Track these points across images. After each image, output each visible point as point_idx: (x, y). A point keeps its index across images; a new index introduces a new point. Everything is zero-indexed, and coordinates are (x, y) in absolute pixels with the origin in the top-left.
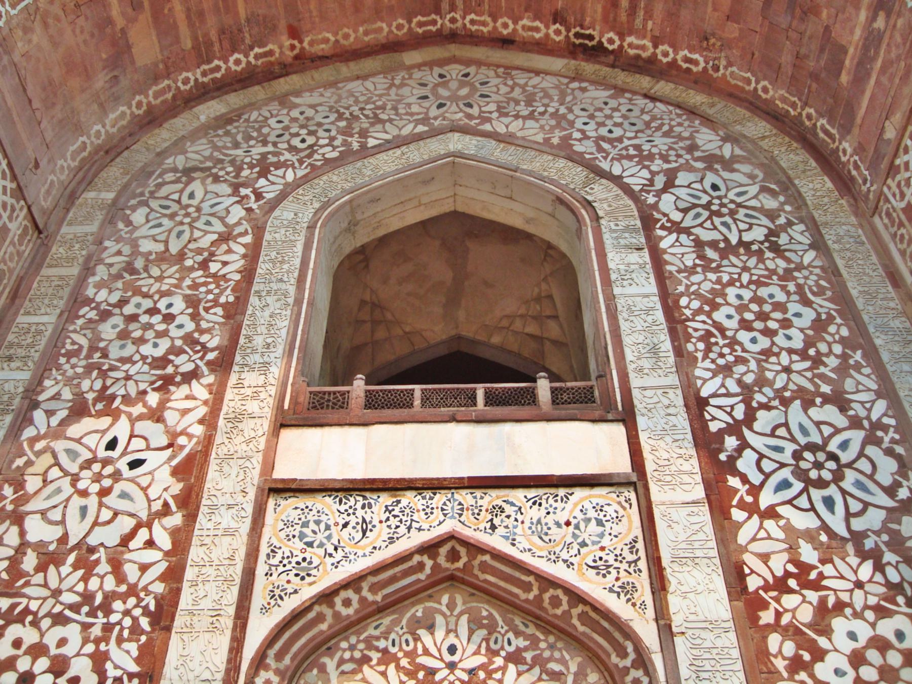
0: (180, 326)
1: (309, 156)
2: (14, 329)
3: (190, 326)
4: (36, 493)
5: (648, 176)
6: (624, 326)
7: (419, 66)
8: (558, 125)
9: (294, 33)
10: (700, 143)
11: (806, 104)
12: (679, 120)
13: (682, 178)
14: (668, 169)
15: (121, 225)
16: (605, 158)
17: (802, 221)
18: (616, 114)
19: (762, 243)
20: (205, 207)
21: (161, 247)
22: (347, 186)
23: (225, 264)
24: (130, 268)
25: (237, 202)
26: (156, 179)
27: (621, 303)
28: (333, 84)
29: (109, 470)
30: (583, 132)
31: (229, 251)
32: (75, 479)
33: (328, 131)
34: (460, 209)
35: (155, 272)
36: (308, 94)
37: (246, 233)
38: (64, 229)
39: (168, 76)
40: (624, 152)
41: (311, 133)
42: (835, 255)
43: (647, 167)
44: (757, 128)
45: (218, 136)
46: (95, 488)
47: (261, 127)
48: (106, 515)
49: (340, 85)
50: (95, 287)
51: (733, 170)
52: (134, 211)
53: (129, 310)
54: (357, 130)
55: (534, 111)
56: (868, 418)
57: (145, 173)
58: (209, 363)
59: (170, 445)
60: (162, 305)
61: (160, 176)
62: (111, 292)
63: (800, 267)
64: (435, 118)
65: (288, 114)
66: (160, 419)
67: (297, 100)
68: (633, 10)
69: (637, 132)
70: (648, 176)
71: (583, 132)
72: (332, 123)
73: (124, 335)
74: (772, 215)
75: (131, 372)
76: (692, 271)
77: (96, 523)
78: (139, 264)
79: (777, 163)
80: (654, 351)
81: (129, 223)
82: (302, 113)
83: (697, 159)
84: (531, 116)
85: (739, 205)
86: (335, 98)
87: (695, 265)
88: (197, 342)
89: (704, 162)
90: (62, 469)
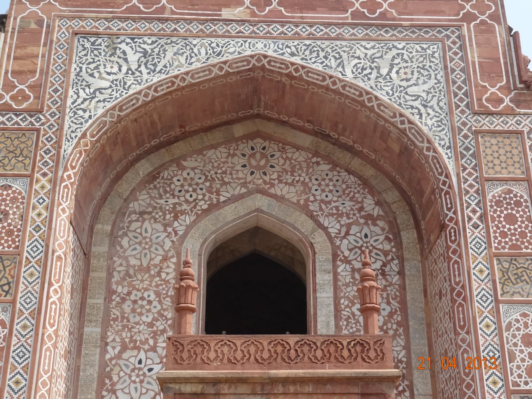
0: (155, 307)
1: (195, 207)
2: (87, 306)
3: (159, 307)
4: (118, 382)
5: (339, 228)
6: (319, 312)
7: (241, 139)
8: (305, 188)
9: (181, 127)
10: (365, 205)
11: (412, 195)
12: (358, 189)
13: (354, 229)
14: (349, 223)
15: (118, 248)
16: (322, 215)
17: (398, 258)
18: (331, 183)
19: (378, 270)
20: (154, 237)
21: (138, 263)
22: (214, 228)
23: (168, 274)
24: (128, 274)
25: (167, 236)
26: (127, 218)
27: (318, 300)
28: (200, 152)
29: (141, 373)
30: (314, 195)
31: (168, 267)
32: (130, 377)
33: (201, 189)
34: (259, 225)
35: (139, 277)
36: (189, 159)
37: (173, 257)
38: (93, 249)
39: (125, 158)
40: (331, 211)
41: (194, 190)
42: (406, 278)
43: (339, 222)
44: (392, 196)
45: (150, 189)
46: (138, 380)
47: (171, 183)
48: (144, 391)
49: (205, 152)
50: (116, 284)
51: (375, 225)
52: (122, 239)
53: (133, 297)
54: (214, 190)
55: (294, 179)
56: (397, 358)
57: (121, 213)
58: (169, 326)
59: (161, 362)
60: (145, 295)
61: (129, 216)
62: (123, 287)
63: (391, 284)
64: (250, 183)
65: (182, 175)
66: (155, 351)
67: (185, 163)
68: (344, 129)
69: (338, 197)
70: (339, 228)
71: (314, 195)
72: (203, 183)
73: (133, 311)
74: (386, 253)
75: (141, 329)
76: (347, 285)
77: (141, 394)
78: (131, 272)
79: (396, 221)
80: (328, 324)
81: (122, 247)
82: (188, 174)
83: (361, 217)
84: (292, 184)
85: (374, 248)
86: (203, 163)
87: (350, 282)
88: (162, 315)
89: (365, 219)
90: (124, 372)
